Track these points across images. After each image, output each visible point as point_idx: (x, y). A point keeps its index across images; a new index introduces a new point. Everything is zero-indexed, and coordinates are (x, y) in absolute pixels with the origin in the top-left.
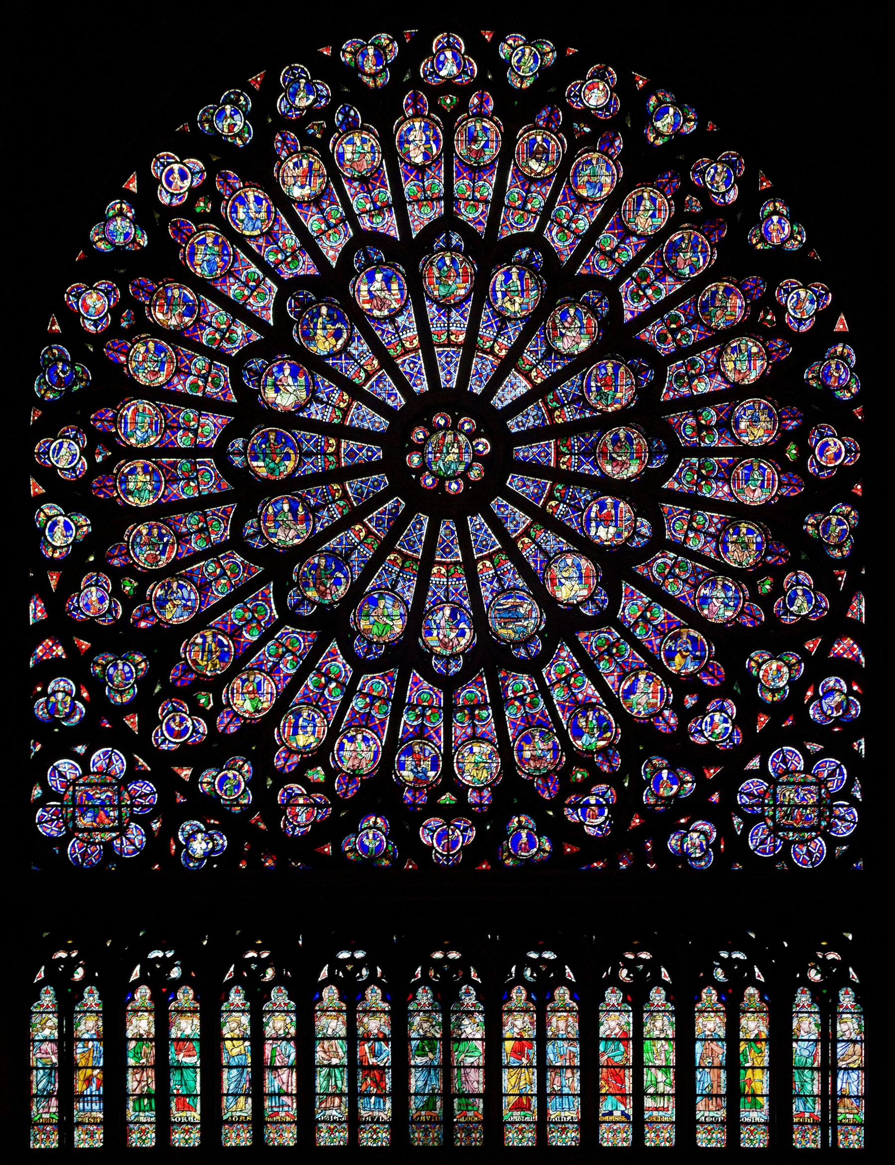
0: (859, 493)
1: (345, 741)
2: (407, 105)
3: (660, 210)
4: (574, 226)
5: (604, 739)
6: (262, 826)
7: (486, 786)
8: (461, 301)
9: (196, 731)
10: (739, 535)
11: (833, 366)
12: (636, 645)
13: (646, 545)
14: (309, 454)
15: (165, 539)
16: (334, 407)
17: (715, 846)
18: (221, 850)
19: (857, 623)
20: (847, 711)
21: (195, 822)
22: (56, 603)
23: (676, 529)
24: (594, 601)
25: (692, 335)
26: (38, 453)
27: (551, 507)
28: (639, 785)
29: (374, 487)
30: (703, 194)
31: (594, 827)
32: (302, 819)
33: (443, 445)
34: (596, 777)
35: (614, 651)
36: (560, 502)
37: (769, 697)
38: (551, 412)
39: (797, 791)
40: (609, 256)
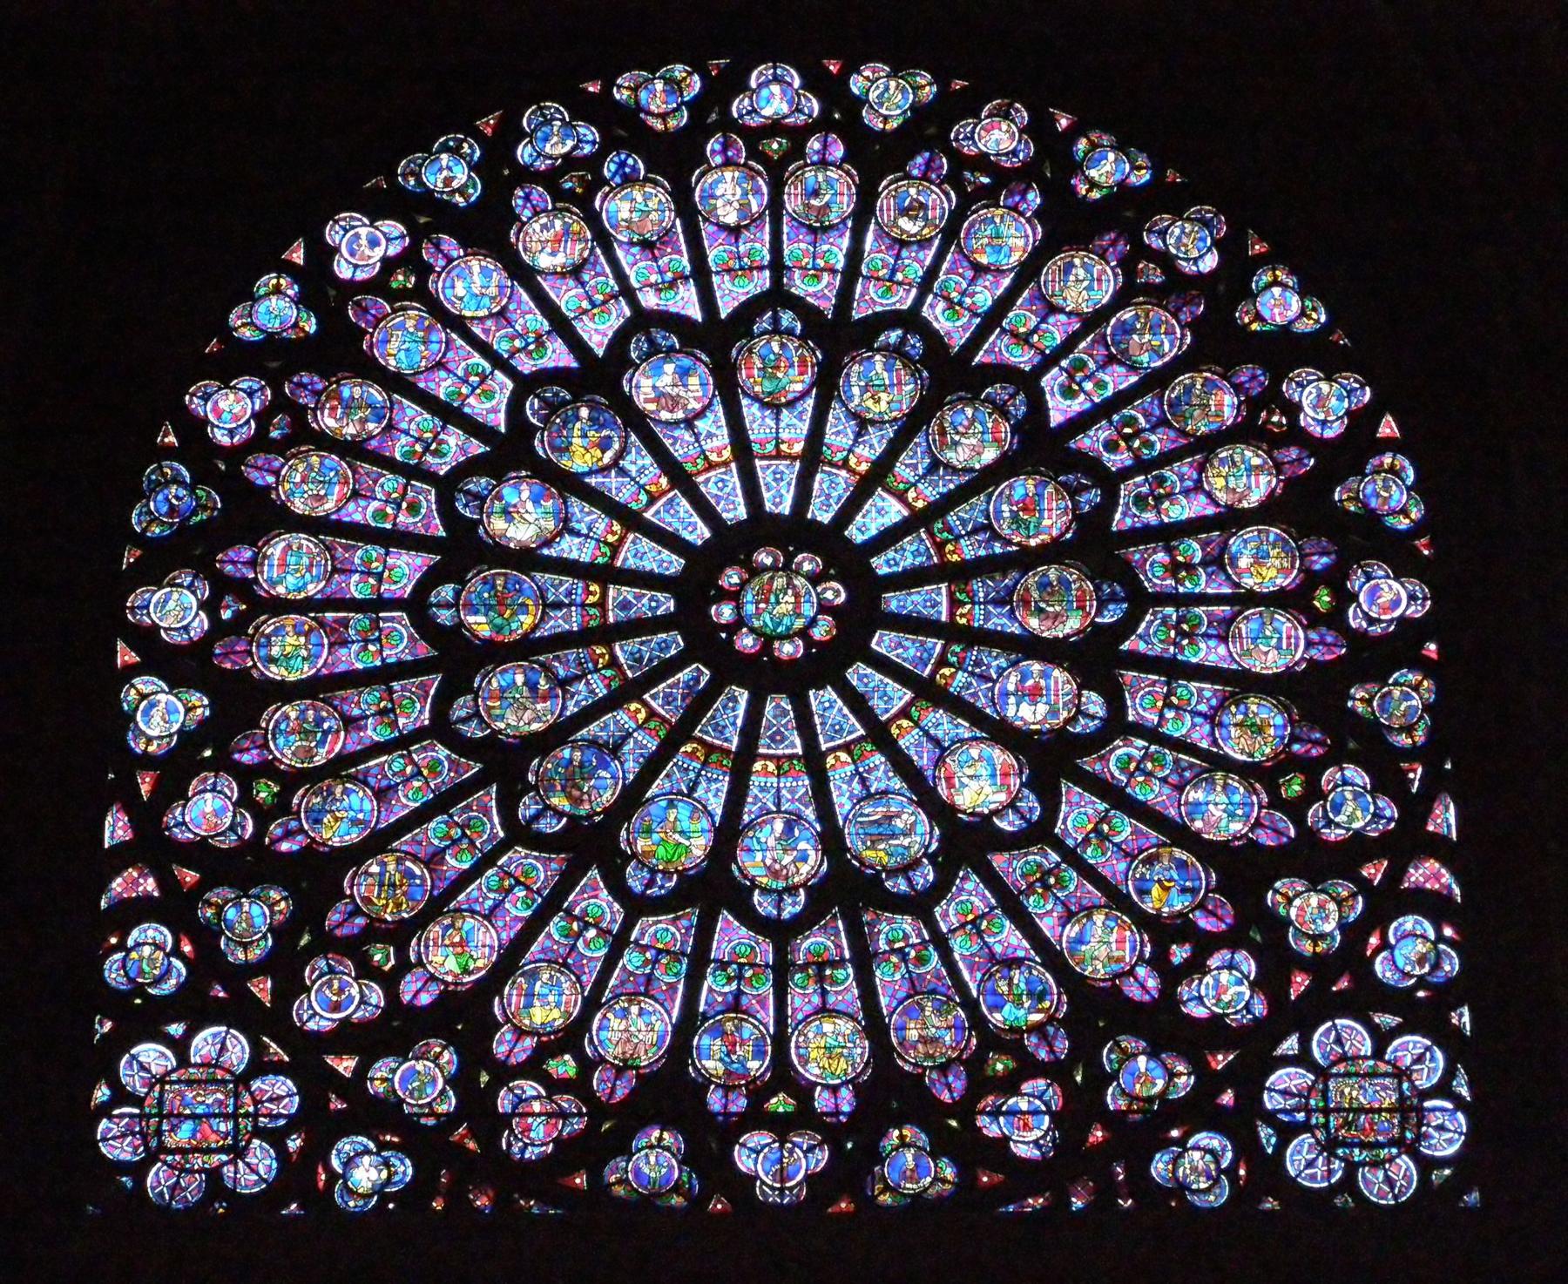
0: (1434, 656)
1: (610, 1015)
2: (713, 152)
3: (1099, 280)
4: (968, 301)
5: (1039, 1011)
6: (471, 1145)
7: (845, 1083)
8: (797, 399)
9: (363, 1001)
10: (1246, 714)
11: (1380, 483)
12: (1089, 873)
13: (1098, 730)
14: (558, 605)
15: (326, 726)
16: (598, 541)
17: (1231, 1172)
18: (401, 1181)
19: (1445, 839)
20: (1436, 966)
21: (360, 1139)
22: (148, 818)
23: (1141, 708)
24: (1017, 810)
25: (1160, 441)
26: (132, 608)
27: (943, 676)
28: (1101, 1079)
29: (661, 650)
30: (1164, 260)
31: (1027, 1143)
32: (539, 1131)
33: (770, 591)
34: (1028, 1067)
35: (1052, 881)
36: (958, 669)
37: (1307, 947)
38: (940, 547)
39: (1361, 1087)
40: (1024, 340)
